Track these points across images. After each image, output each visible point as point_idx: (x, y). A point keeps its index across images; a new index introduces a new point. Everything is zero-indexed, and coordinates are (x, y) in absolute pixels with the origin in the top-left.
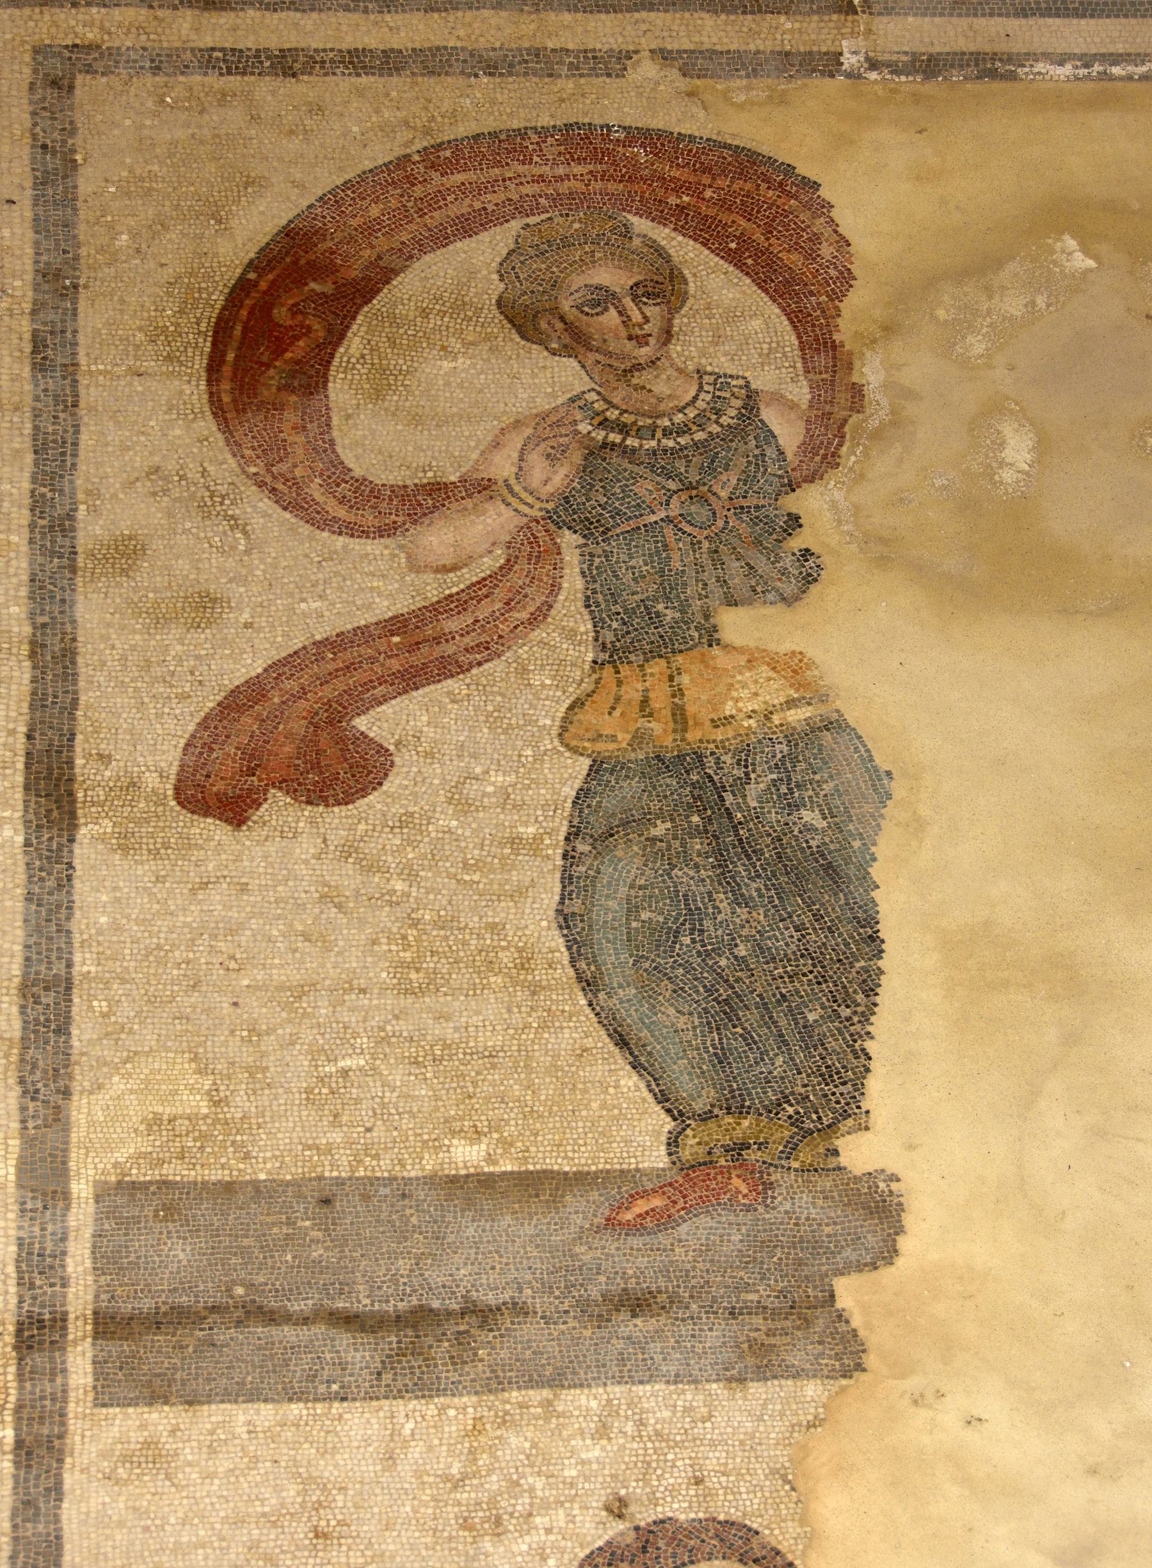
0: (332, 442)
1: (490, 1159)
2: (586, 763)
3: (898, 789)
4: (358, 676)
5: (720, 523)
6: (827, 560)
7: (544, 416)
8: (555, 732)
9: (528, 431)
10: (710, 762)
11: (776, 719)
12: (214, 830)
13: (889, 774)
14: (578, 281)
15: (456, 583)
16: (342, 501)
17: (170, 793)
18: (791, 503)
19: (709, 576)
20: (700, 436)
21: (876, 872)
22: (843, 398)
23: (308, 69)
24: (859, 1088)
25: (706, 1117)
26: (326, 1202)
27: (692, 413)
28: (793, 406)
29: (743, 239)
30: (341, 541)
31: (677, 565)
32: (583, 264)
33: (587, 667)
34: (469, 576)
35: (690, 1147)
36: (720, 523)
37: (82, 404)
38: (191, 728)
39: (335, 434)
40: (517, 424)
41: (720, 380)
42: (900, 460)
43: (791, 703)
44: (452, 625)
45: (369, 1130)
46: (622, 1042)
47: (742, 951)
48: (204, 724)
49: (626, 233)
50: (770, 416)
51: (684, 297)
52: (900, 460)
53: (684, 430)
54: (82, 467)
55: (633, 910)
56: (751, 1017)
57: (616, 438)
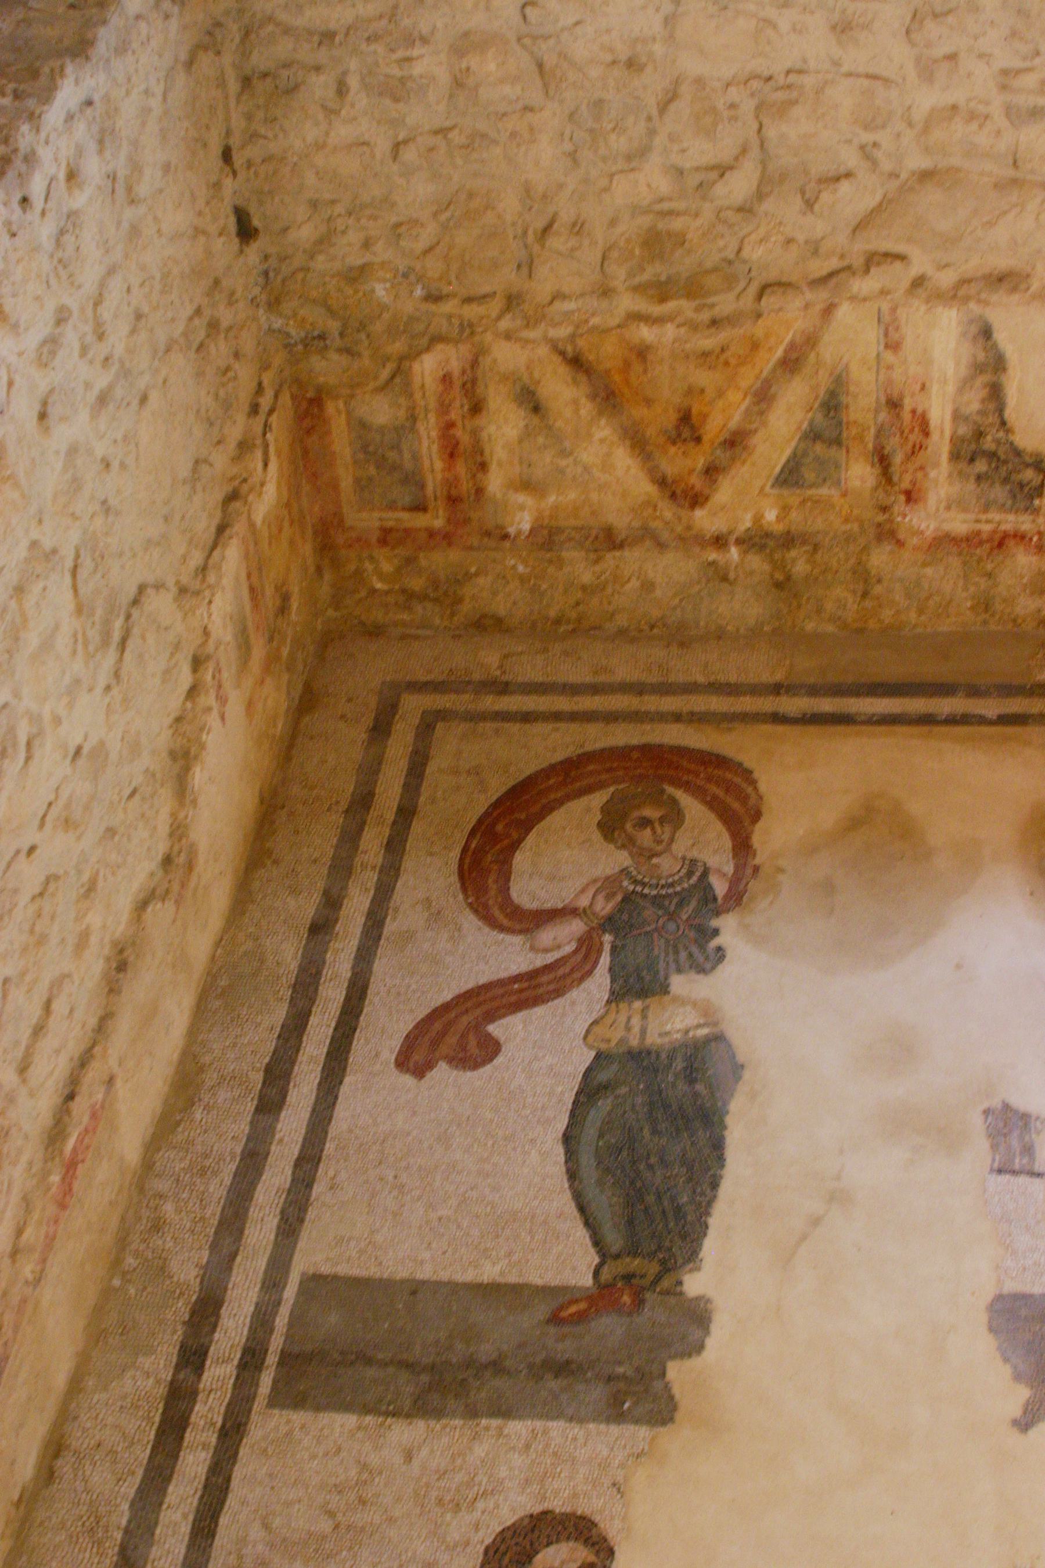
0: (509, 888)
1: (502, 1273)
2: (593, 1053)
3: (747, 1075)
4: (495, 1004)
5: (680, 932)
6: (729, 954)
7: (607, 878)
8: (582, 1036)
9: (599, 884)
10: (653, 1056)
11: (691, 1034)
12: (408, 1080)
13: (742, 1066)
14: (636, 814)
15: (550, 958)
16: (507, 915)
17: (393, 1061)
18: (715, 923)
19: (671, 958)
20: (678, 889)
21: (729, 1120)
22: (749, 871)
23: (536, 720)
25: (617, 1256)
26: (414, 1293)
27: (676, 878)
29: (715, 798)
30: (502, 936)
31: (656, 952)
32: (638, 807)
33: (604, 1002)
34: (556, 955)
35: (606, 1275)
36: (680, 932)
37: (402, 868)
38: (411, 1027)
39: (511, 884)
40: (595, 881)
41: (693, 862)
42: (772, 903)
43: (699, 1026)
44: (545, 979)
45: (444, 1253)
46: (582, 1209)
47: (653, 1160)
48: (416, 1027)
49: (663, 791)
51: (683, 822)
52: (772, 903)
53: (672, 885)
54: (394, 897)
55: (601, 1136)
56: (651, 1199)
57: (639, 889)
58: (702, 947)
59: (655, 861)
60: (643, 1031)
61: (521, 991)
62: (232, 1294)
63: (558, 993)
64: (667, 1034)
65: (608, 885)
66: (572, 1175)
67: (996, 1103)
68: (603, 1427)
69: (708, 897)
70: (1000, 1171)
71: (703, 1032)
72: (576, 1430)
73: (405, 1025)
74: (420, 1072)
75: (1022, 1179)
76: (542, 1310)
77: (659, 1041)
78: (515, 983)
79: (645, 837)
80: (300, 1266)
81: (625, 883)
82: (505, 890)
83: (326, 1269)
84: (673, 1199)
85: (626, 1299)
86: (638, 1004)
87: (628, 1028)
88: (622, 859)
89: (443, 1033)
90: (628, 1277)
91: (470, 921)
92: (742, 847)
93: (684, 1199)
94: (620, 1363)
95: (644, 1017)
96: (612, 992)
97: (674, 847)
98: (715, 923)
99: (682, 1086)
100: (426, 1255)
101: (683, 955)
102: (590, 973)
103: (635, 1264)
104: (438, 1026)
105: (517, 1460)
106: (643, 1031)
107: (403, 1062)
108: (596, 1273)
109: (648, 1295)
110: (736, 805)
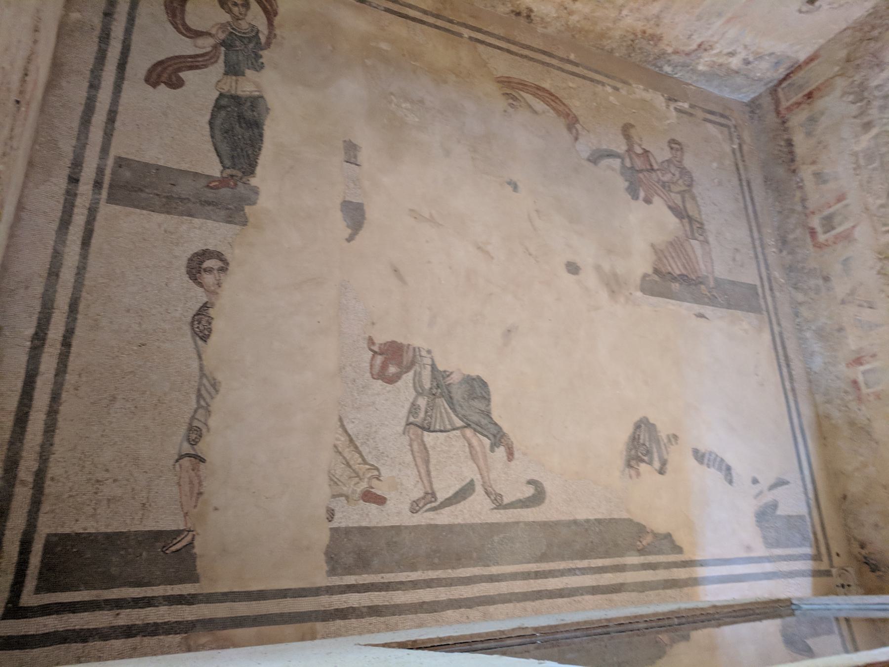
2: (217, 93)
3: (271, 113)
12: (150, 88)
16: (185, 30)
18: (261, 53)
21: (265, 127)
24: (255, 169)
25: (228, 168)
27: (247, 31)
28: (264, 34)
30: (183, 37)
34: (204, 51)
35: (225, 175)
43: (256, 91)
44: (200, 59)
46: (216, 149)
47: (240, 137)
50: (261, 35)
56: (239, 150)
58: (257, 61)
59: (240, 22)
60: (236, 88)
61: (192, 62)
62: (87, 159)
63: (206, 66)
64: (244, 91)
65: (223, 27)
66: (212, 137)
67: (347, 139)
68: (225, 224)
69: (258, 43)
70: (347, 162)
71: (257, 93)
72: (216, 224)
73: (148, 65)
74: (154, 85)
75: (353, 166)
76: (203, 182)
77: (242, 93)
78: (189, 58)
79: (236, 10)
80: (113, 152)
81: (229, 28)
82: (183, 19)
83: (124, 156)
84: (247, 152)
85: (232, 183)
86: (234, 78)
87: (231, 87)
88: (227, 18)
89: (162, 72)
90: (232, 176)
91: (170, 27)
92: (270, 24)
93: (250, 152)
94: (229, 204)
95: (237, 83)
96: (226, 71)
97: (246, 18)
98: (261, 53)
99: (250, 113)
100: (161, 156)
101: (250, 62)
102: (216, 62)
103: (234, 172)
104: (160, 69)
105: (197, 231)
106: (236, 88)
107: (147, 80)
108: (222, 172)
109: (239, 184)
110: (269, 7)
